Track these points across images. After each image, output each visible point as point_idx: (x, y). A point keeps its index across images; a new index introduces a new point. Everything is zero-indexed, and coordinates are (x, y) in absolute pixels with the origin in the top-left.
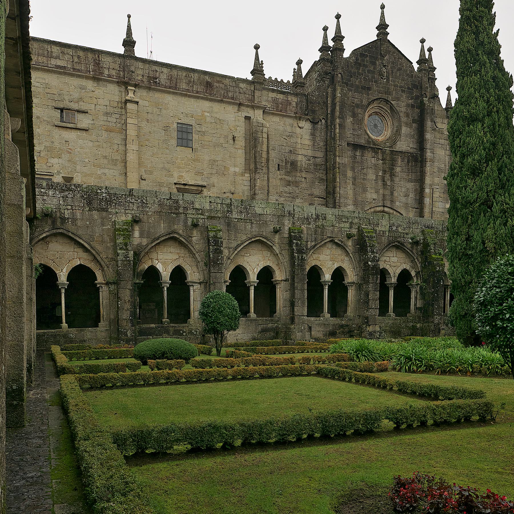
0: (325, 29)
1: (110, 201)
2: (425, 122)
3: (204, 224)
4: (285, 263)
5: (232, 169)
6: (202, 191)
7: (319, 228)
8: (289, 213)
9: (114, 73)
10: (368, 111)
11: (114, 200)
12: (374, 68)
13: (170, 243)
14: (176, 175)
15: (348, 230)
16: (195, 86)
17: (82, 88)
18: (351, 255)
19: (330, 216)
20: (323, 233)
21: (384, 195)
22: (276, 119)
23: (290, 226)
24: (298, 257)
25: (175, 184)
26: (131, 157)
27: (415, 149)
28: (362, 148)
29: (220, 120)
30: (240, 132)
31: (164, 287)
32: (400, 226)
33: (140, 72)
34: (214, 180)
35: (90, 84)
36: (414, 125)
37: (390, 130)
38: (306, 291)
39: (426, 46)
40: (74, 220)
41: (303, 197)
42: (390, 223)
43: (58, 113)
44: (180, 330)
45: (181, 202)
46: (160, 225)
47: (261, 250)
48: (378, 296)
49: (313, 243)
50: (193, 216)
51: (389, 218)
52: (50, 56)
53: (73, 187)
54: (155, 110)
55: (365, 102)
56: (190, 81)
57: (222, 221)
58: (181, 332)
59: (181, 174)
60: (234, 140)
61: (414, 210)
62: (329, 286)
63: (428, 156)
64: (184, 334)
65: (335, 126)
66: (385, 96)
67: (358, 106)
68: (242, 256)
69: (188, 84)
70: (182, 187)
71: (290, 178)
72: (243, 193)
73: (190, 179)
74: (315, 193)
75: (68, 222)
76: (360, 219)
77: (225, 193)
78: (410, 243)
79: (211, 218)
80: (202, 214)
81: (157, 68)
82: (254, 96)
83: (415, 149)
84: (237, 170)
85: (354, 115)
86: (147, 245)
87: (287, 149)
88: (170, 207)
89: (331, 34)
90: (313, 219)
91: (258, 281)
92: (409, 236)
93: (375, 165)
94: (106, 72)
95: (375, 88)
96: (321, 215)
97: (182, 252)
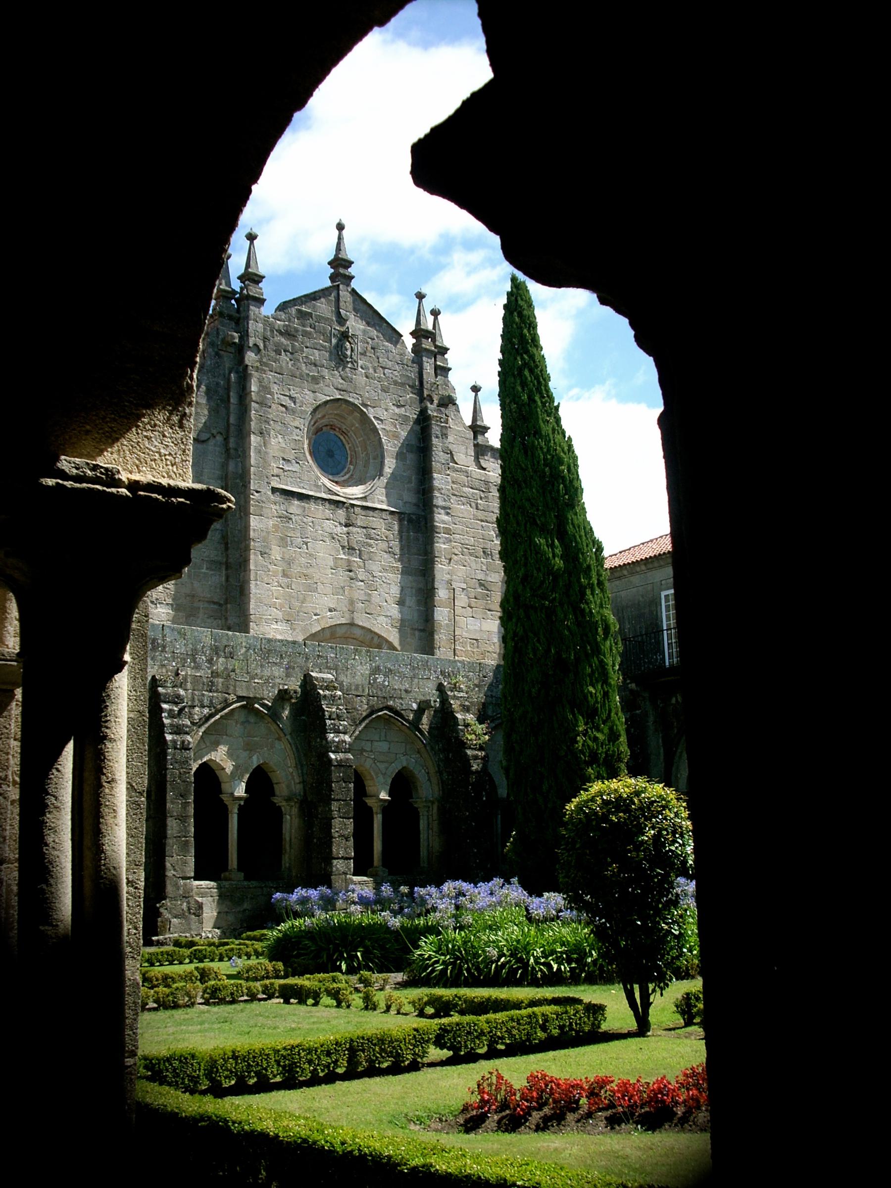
39: (428, 305)
48: (350, 829)
49: (206, 711)
51: (370, 656)
62: (241, 808)
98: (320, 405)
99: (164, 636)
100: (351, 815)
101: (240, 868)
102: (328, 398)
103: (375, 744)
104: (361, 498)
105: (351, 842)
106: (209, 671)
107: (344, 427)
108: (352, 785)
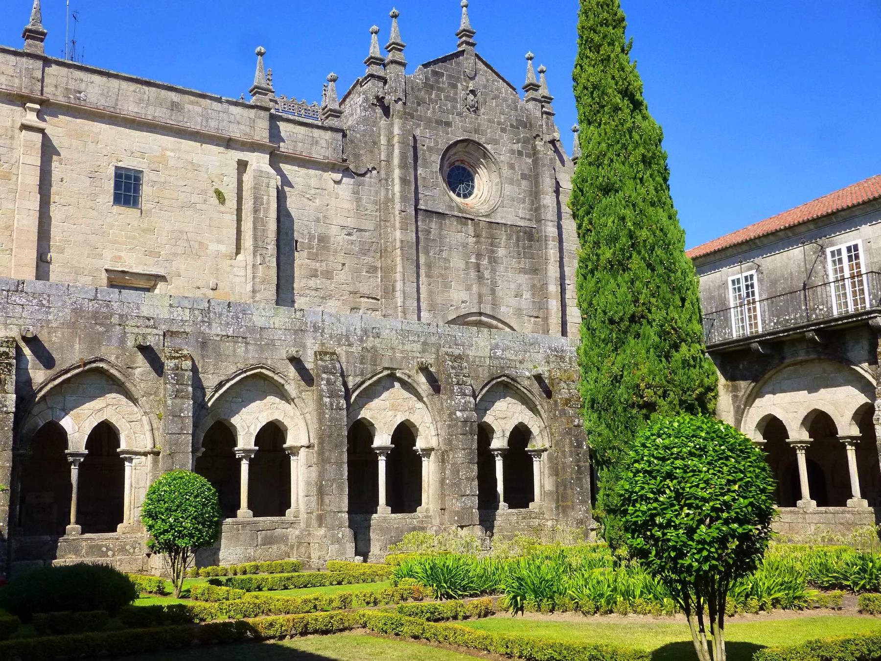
4: (307, 415)
5: (213, 247)
7: (368, 351)
10: (449, 158)
15: (419, 355)
18: (425, 399)
19: (387, 331)
21: (480, 296)
24: (332, 405)
25: (107, 270)
34: (180, 264)
36: (524, 183)
38: (346, 466)
41: (341, 296)
44: (102, 546)
45: (115, 305)
46: (72, 347)
50: (136, 330)
58: (104, 549)
64: (110, 553)
65: (393, 180)
71: (317, 264)
73: (135, 264)
74: (361, 289)
76: (440, 337)
77: (199, 288)
84: (223, 248)
90: (357, 336)
91: (257, 448)
93: (465, 245)
96: (371, 330)
98: (451, 145)
100: (476, 461)
101: (388, 504)
102: (459, 139)
104: (486, 216)
105: (476, 483)
106: (360, 348)
107: (471, 162)
108: (476, 437)
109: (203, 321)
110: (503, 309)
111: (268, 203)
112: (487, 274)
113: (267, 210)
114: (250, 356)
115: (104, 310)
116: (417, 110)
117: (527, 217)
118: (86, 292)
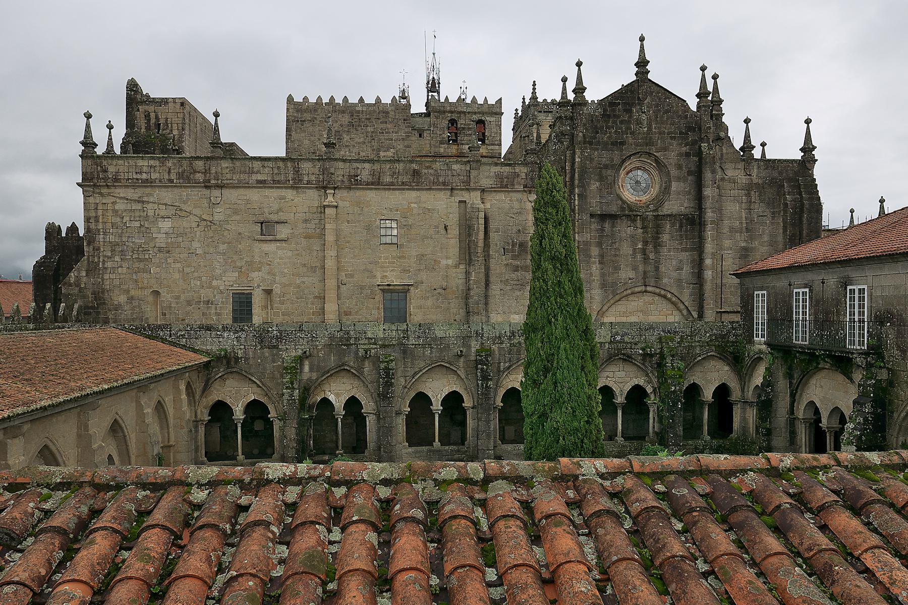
0: (564, 80)
1: (281, 338)
2: (703, 175)
3: (377, 354)
5: (444, 262)
6: (409, 289)
7: (515, 346)
8: (477, 333)
9: (313, 178)
11: (285, 336)
12: (630, 117)
13: (343, 374)
14: (379, 275)
16: (400, 177)
17: (282, 198)
20: (520, 352)
21: (645, 273)
22: (502, 196)
23: (478, 347)
24: (483, 385)
26: (330, 263)
27: (692, 208)
28: (613, 217)
29: (429, 210)
30: (453, 220)
31: (337, 419)
32: (626, 334)
33: (340, 172)
34: (423, 276)
35: (289, 194)
36: (690, 178)
37: (657, 186)
39: (709, 74)
40: (247, 359)
42: (611, 332)
43: (258, 228)
45: (352, 333)
46: (330, 359)
47: (446, 374)
49: (507, 365)
52: (252, 172)
53: (246, 327)
54: (356, 209)
55: (617, 160)
56: (394, 173)
57: (397, 348)
59: (385, 274)
60: (446, 230)
61: (691, 286)
63: (709, 217)
66: (647, 149)
67: (606, 167)
68: (423, 381)
69: (392, 176)
70: (387, 287)
72: (457, 287)
75: (241, 361)
77: (435, 289)
78: (641, 355)
79: (384, 346)
80: (375, 344)
81: (358, 165)
82: (470, 176)
83: (692, 208)
84: (450, 262)
85: (601, 179)
86: (317, 379)
87: (515, 229)
88: (341, 338)
89: (571, 85)
92: (640, 345)
93: (632, 236)
94: (306, 178)
95: (631, 140)
97: (356, 382)
99: (482, 329)
103: (616, 373)
109: (404, 337)
110: (665, 280)
111: (478, 228)
112: (652, 256)
113: (477, 234)
114: (434, 355)
115: (346, 336)
116: (596, 138)
117: (692, 205)
118: (336, 327)
